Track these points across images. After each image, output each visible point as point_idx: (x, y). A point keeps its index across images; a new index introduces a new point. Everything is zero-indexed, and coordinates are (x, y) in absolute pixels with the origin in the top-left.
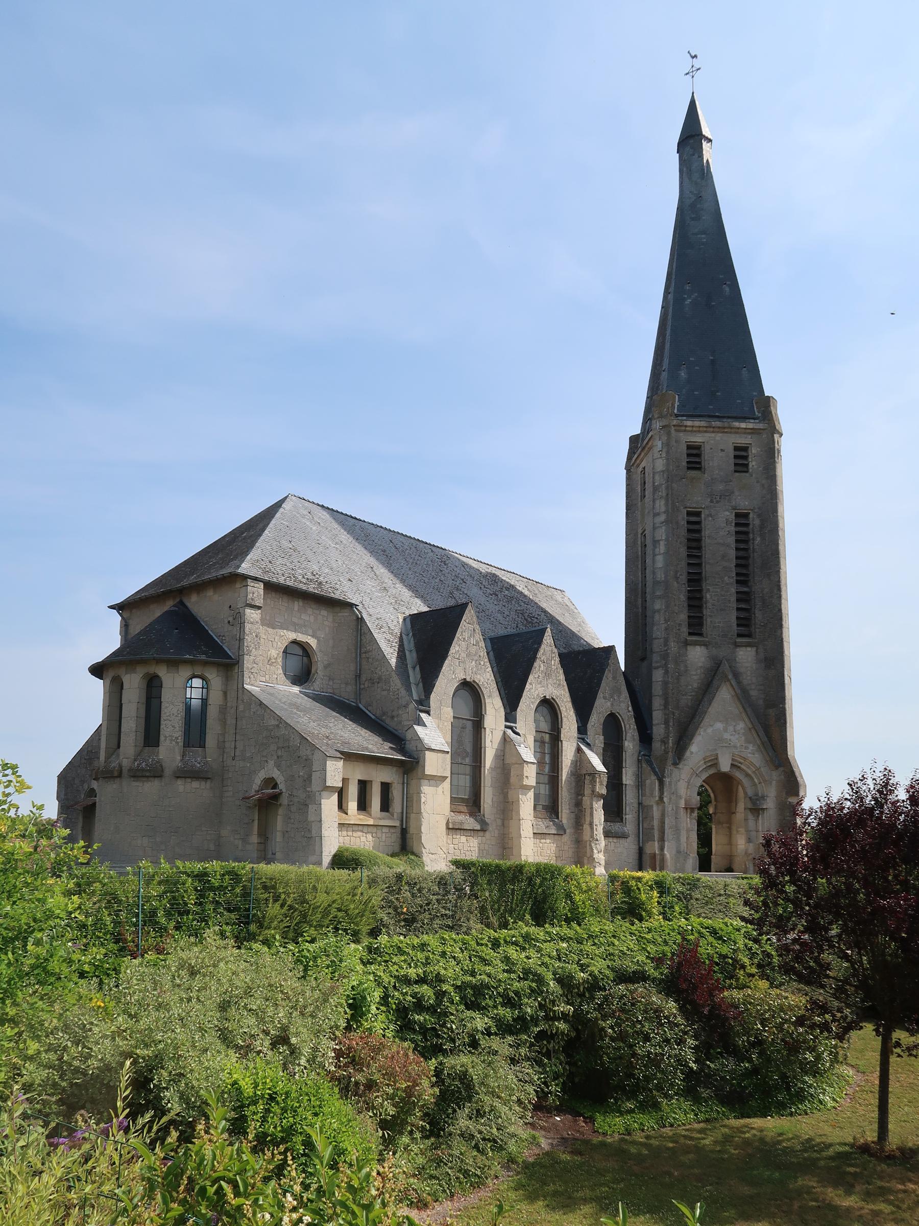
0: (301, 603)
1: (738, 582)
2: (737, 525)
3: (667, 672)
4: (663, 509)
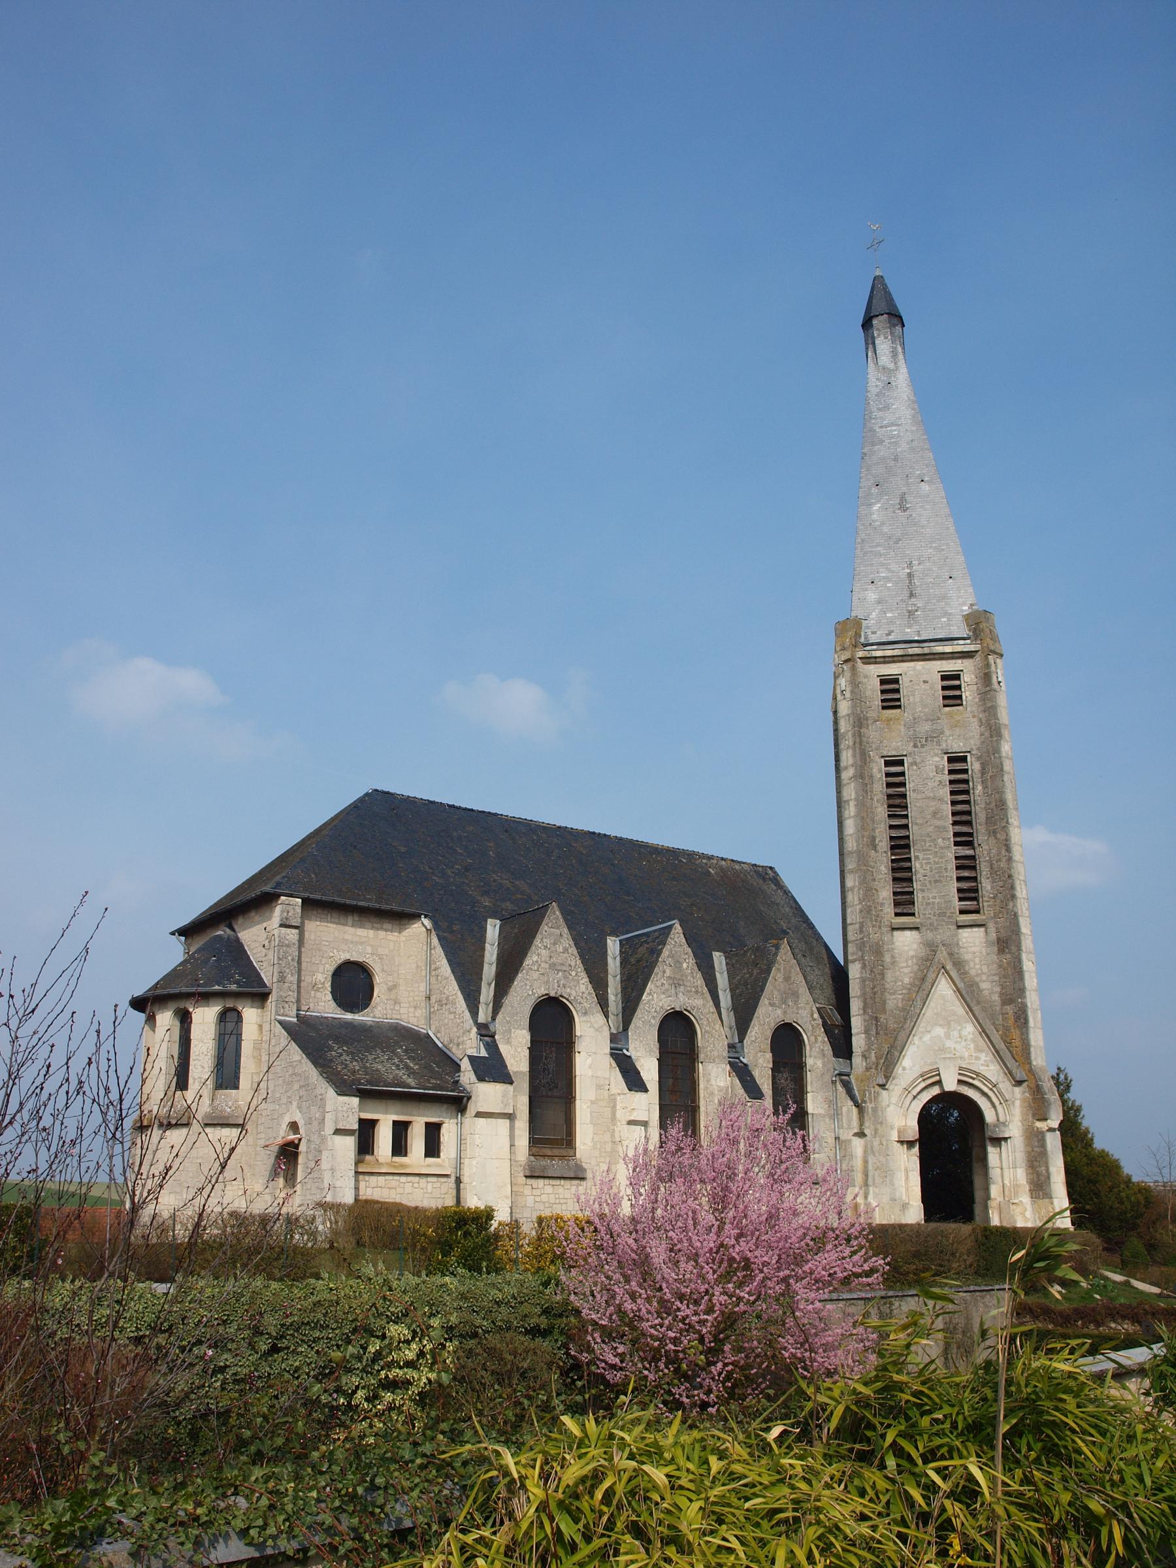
0: (356, 918)
1: (956, 844)
2: (951, 772)
3: (864, 967)
4: (851, 761)
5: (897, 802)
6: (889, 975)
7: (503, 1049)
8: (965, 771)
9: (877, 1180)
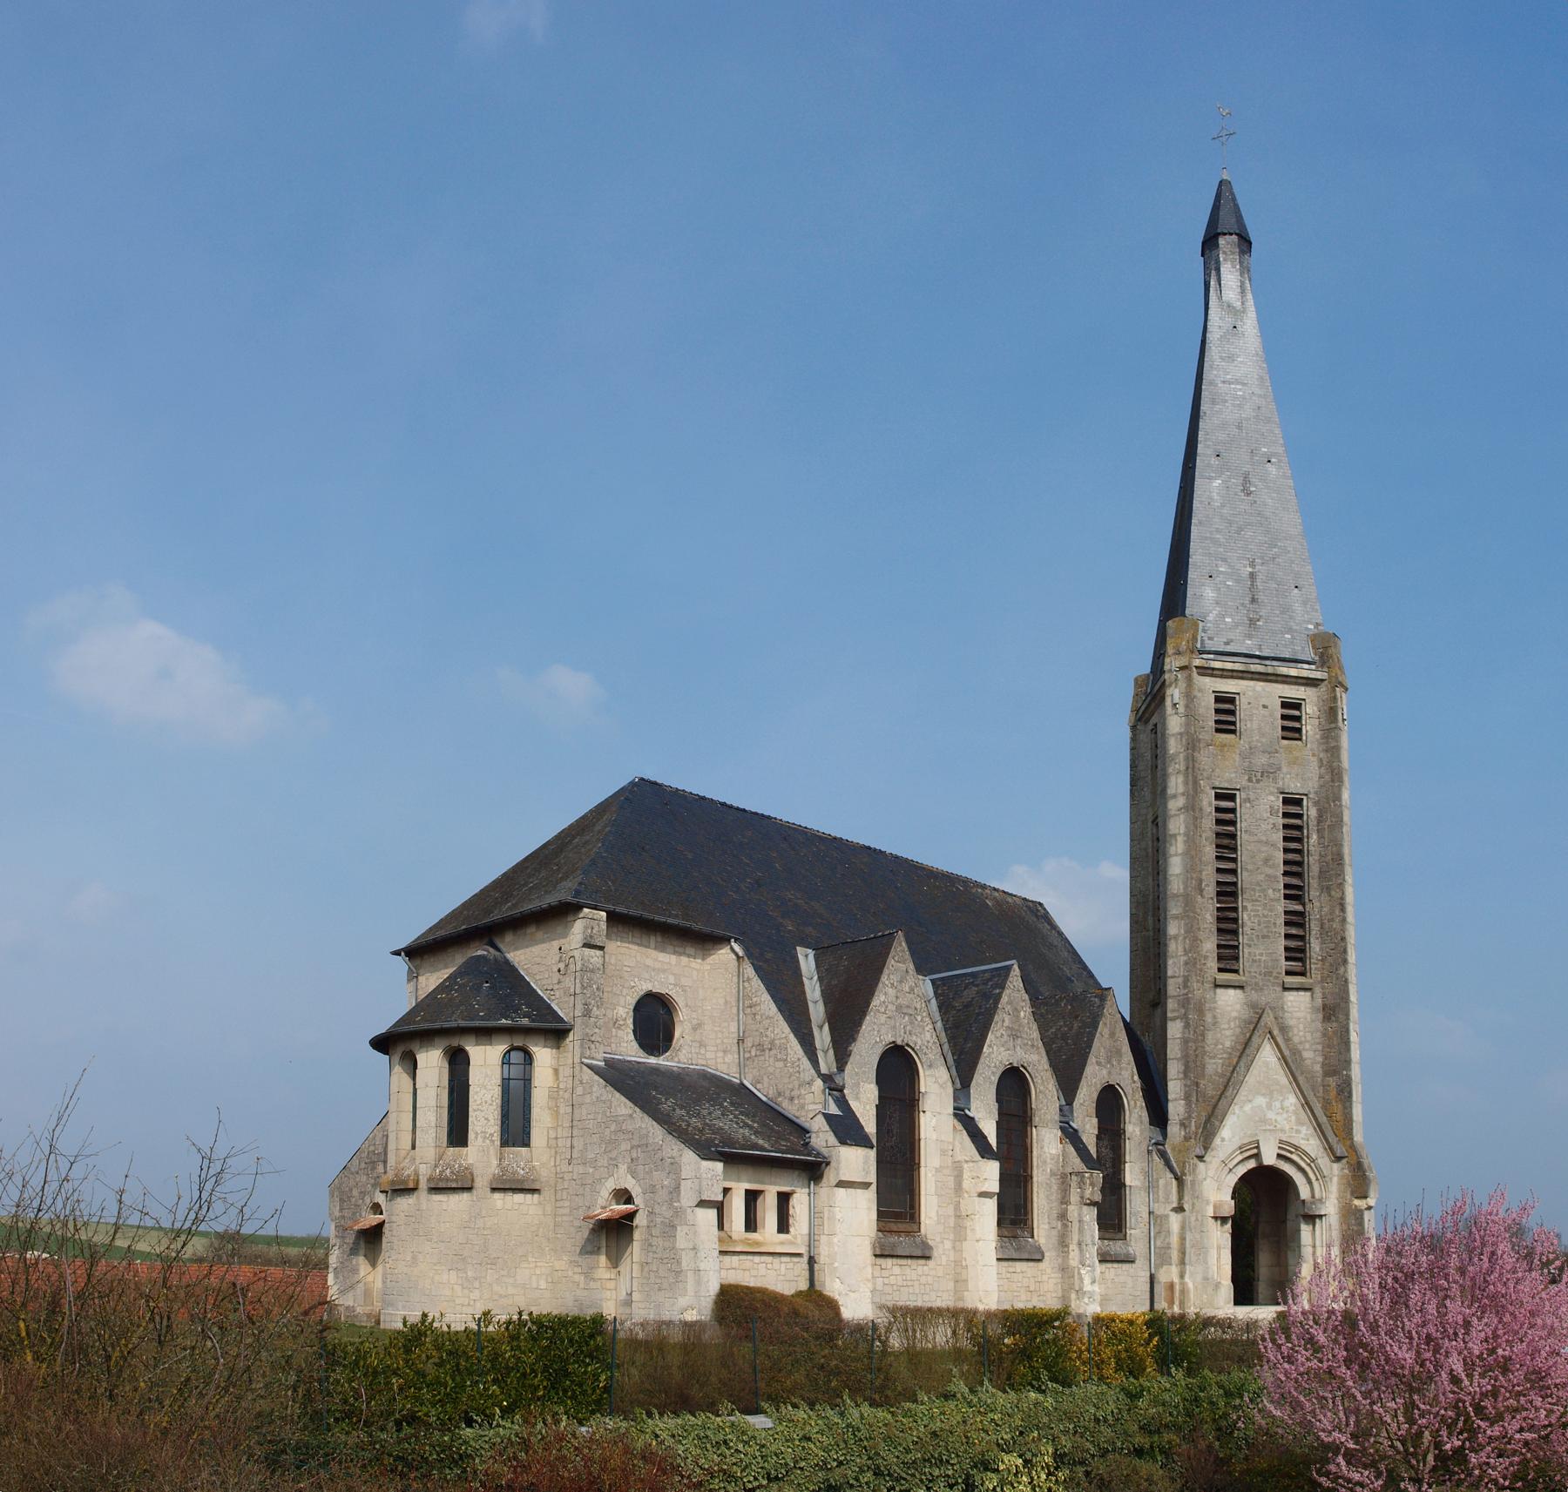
1: (1286, 897)
3: (1187, 1026)
5: (1227, 843)
6: (1210, 1036)
7: (854, 1104)
8: (1300, 816)
9: (1194, 1258)
